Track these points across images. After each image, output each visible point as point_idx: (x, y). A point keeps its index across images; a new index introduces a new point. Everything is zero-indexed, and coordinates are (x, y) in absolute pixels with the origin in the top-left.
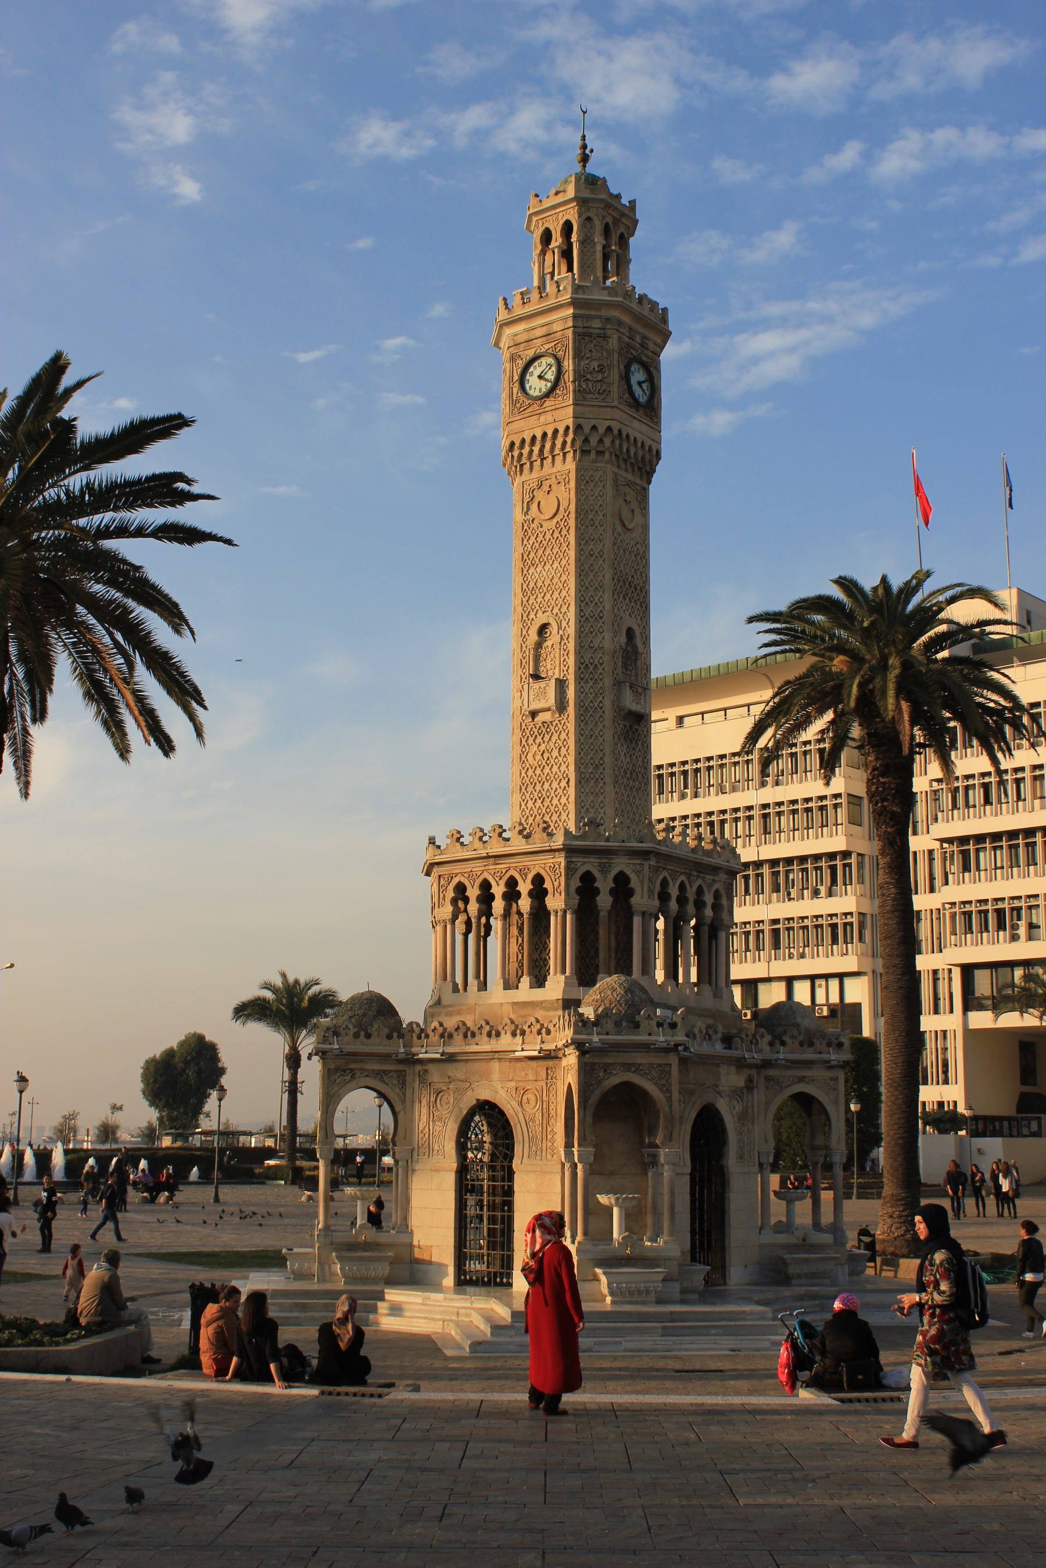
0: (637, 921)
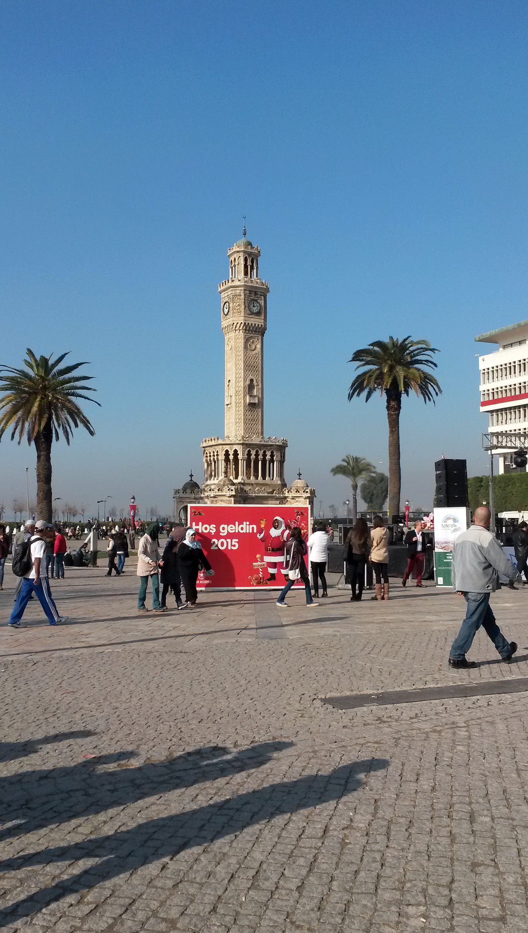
0: (240, 461)
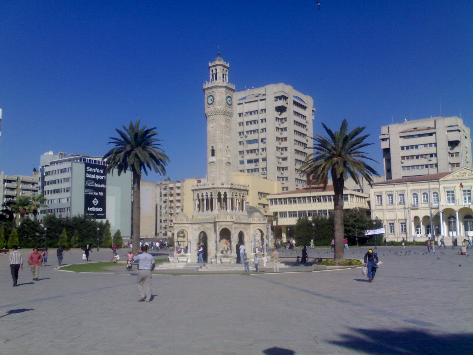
0: (228, 200)
